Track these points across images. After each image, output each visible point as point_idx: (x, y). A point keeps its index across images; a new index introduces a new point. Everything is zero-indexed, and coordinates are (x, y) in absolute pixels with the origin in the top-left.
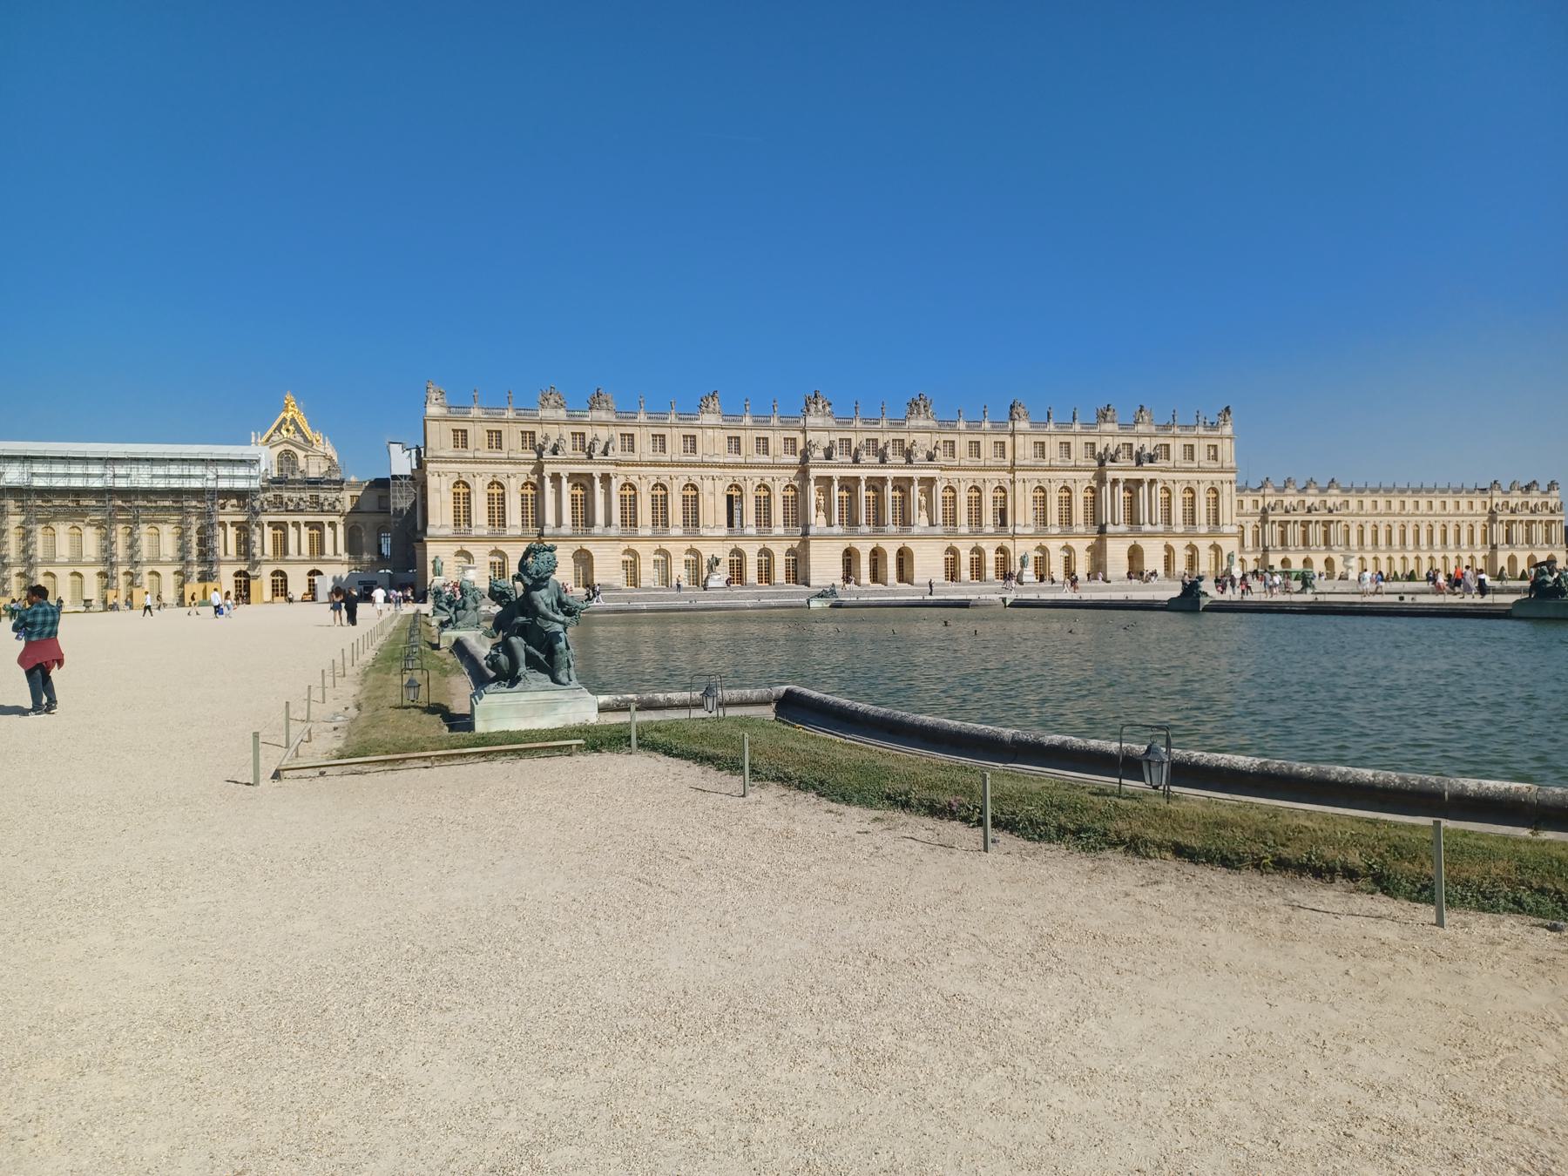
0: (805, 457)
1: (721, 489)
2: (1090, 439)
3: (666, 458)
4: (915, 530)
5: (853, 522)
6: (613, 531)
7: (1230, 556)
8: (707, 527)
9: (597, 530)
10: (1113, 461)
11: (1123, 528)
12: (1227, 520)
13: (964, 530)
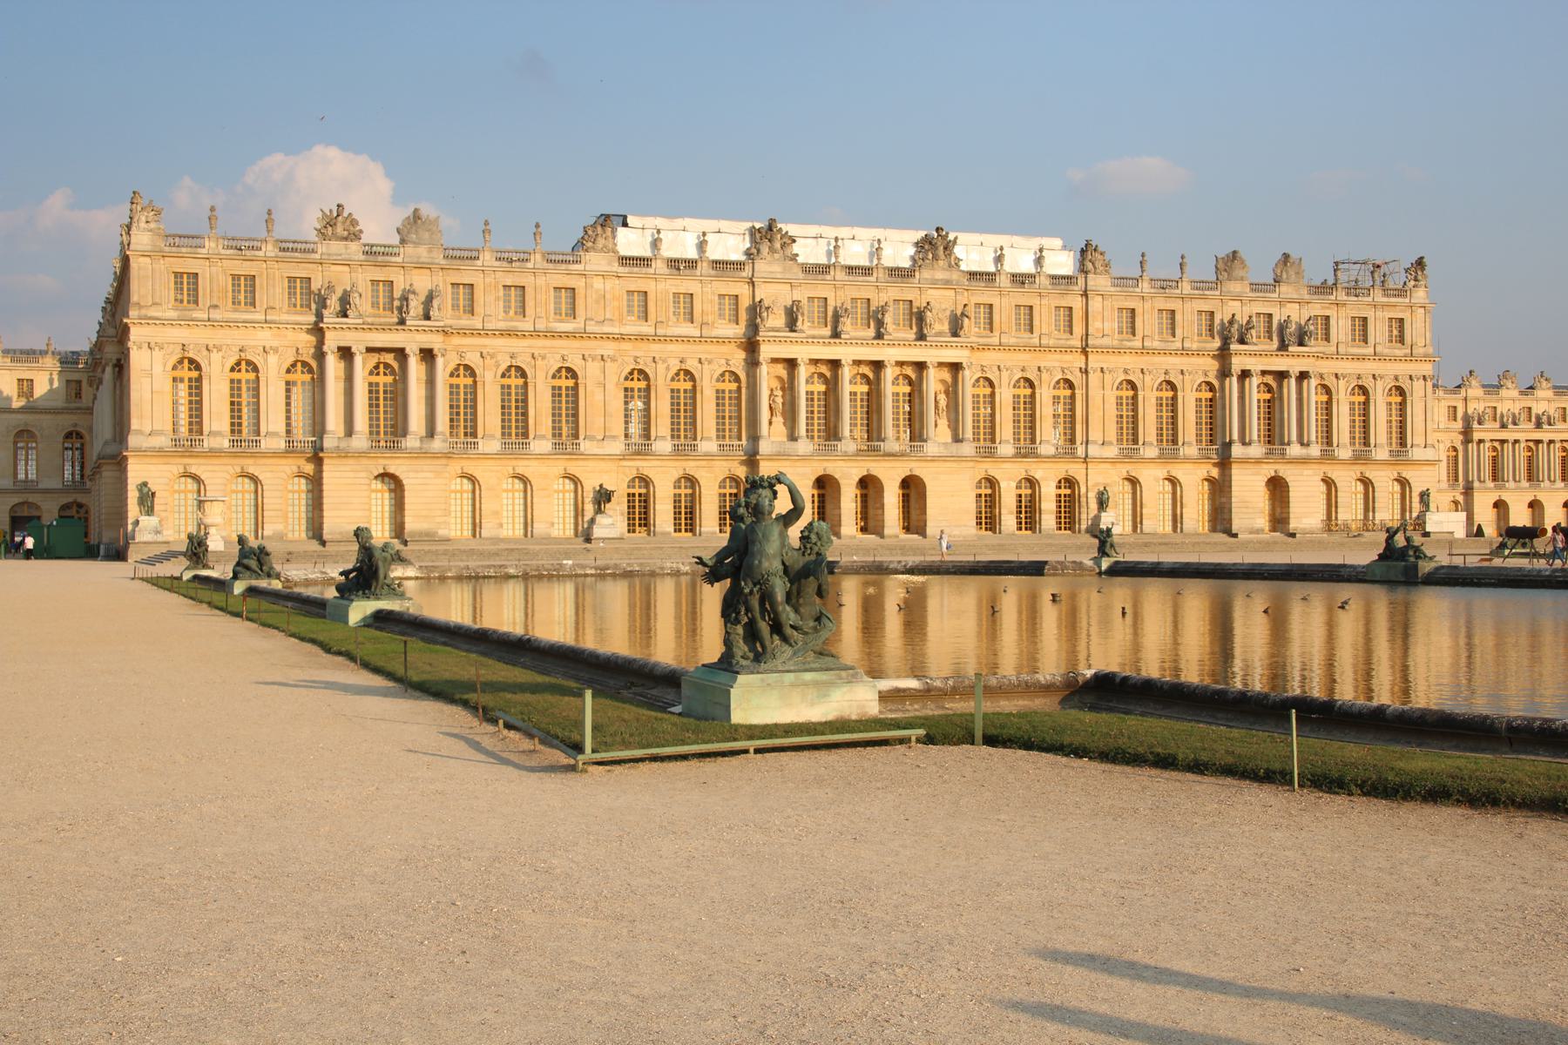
0: (753, 328)
1: (615, 374)
3: (527, 325)
4: (931, 448)
5: (832, 433)
6: (437, 444)
7: (1424, 496)
8: (592, 438)
9: (411, 442)
10: (1242, 341)
11: (1257, 450)
12: (1419, 440)
13: (1006, 449)
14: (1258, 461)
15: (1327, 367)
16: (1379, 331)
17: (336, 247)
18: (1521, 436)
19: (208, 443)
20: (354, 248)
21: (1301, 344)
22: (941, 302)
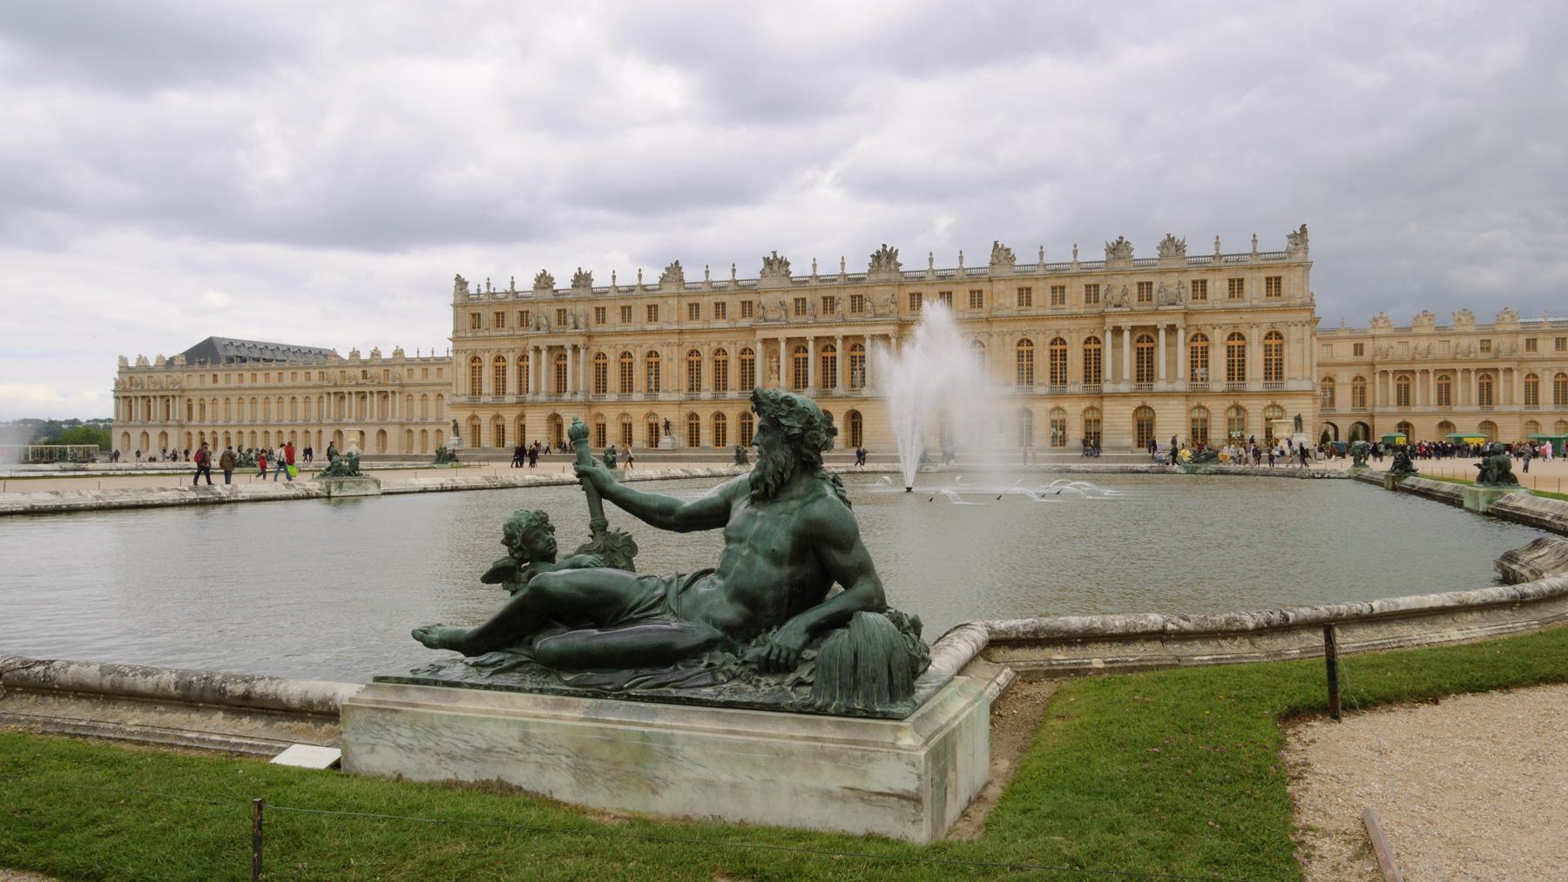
2: (1091, 281)
7: (1298, 420)
9: (567, 396)
14: (1125, 396)
15: (1201, 320)
17: (541, 293)
19: (483, 399)
20: (548, 292)
22: (880, 295)
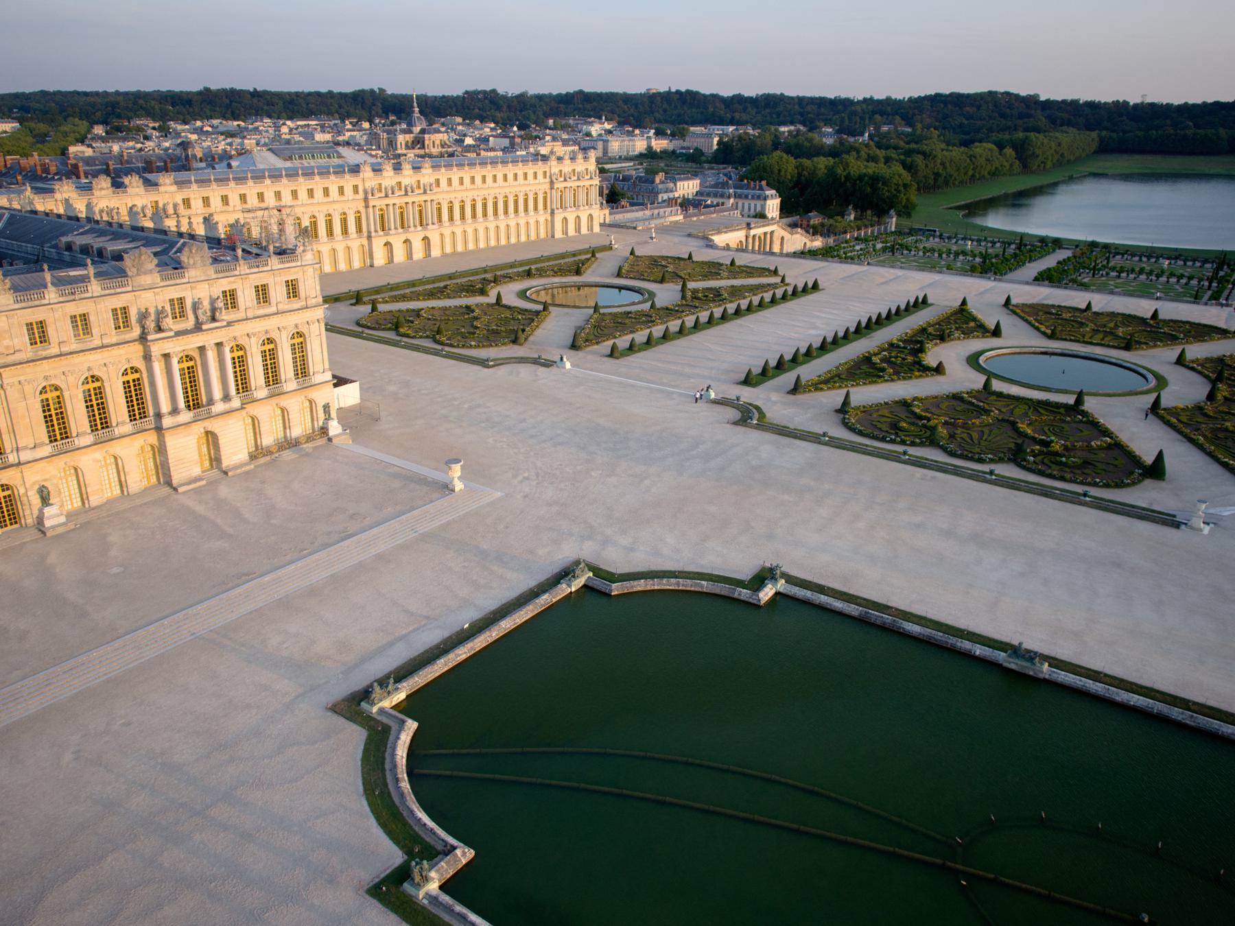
10: (159, 329)
11: (185, 416)
16: (278, 293)
18: (396, 201)
21: (214, 319)
